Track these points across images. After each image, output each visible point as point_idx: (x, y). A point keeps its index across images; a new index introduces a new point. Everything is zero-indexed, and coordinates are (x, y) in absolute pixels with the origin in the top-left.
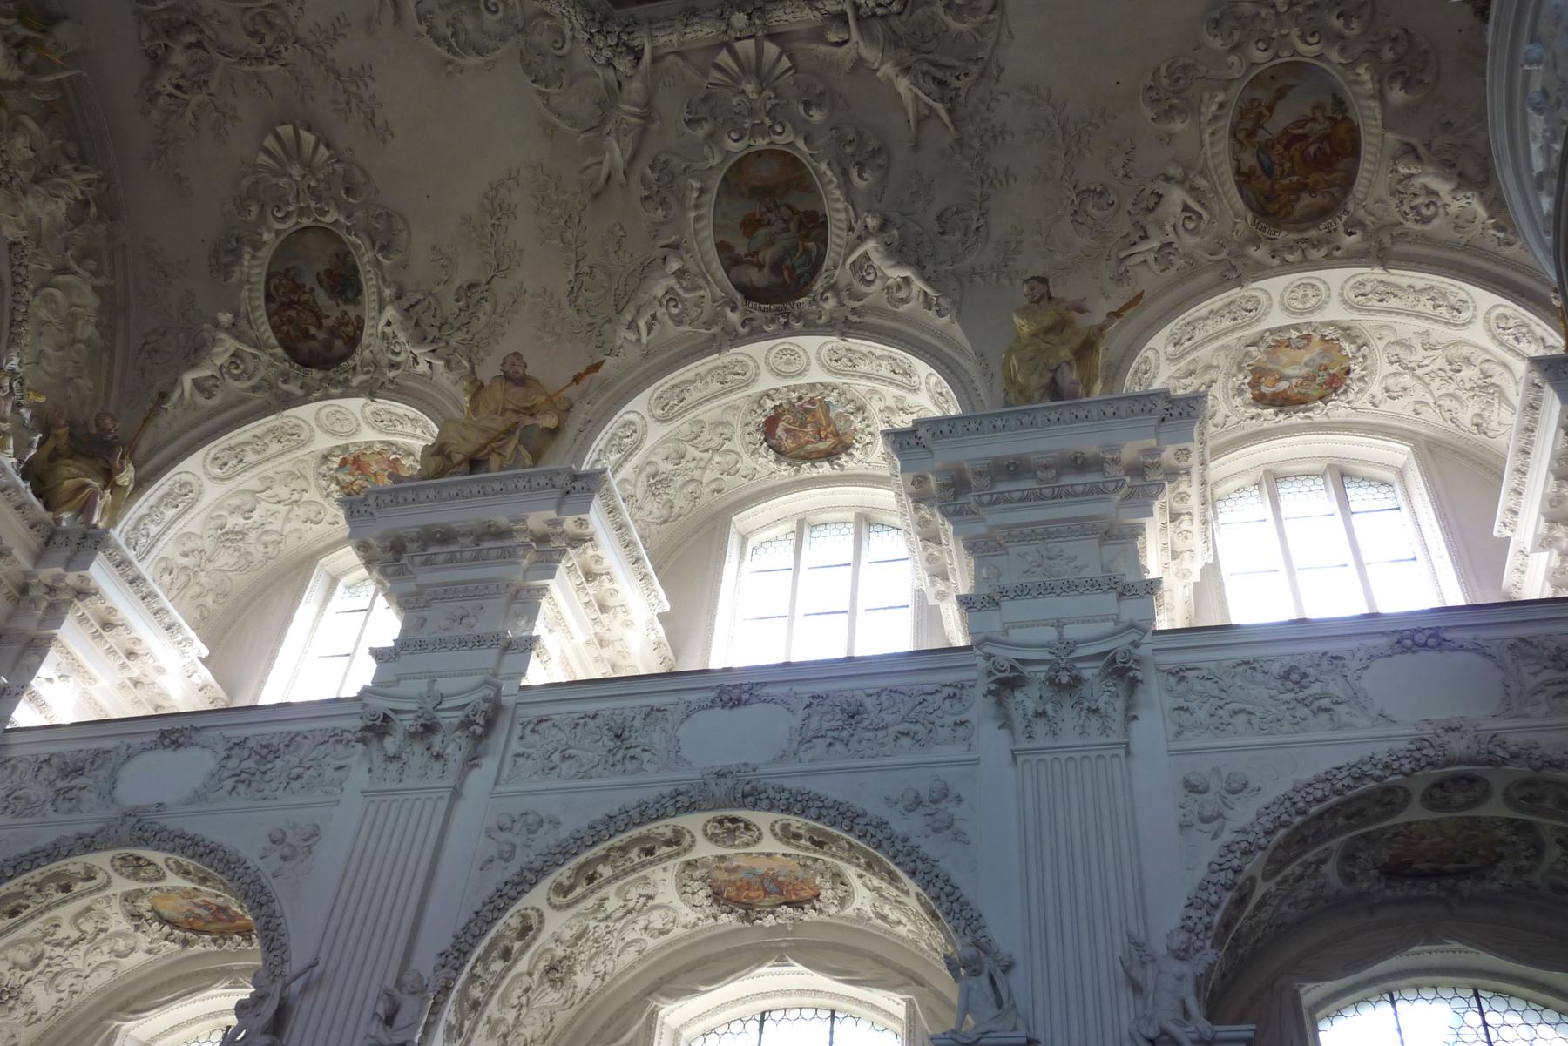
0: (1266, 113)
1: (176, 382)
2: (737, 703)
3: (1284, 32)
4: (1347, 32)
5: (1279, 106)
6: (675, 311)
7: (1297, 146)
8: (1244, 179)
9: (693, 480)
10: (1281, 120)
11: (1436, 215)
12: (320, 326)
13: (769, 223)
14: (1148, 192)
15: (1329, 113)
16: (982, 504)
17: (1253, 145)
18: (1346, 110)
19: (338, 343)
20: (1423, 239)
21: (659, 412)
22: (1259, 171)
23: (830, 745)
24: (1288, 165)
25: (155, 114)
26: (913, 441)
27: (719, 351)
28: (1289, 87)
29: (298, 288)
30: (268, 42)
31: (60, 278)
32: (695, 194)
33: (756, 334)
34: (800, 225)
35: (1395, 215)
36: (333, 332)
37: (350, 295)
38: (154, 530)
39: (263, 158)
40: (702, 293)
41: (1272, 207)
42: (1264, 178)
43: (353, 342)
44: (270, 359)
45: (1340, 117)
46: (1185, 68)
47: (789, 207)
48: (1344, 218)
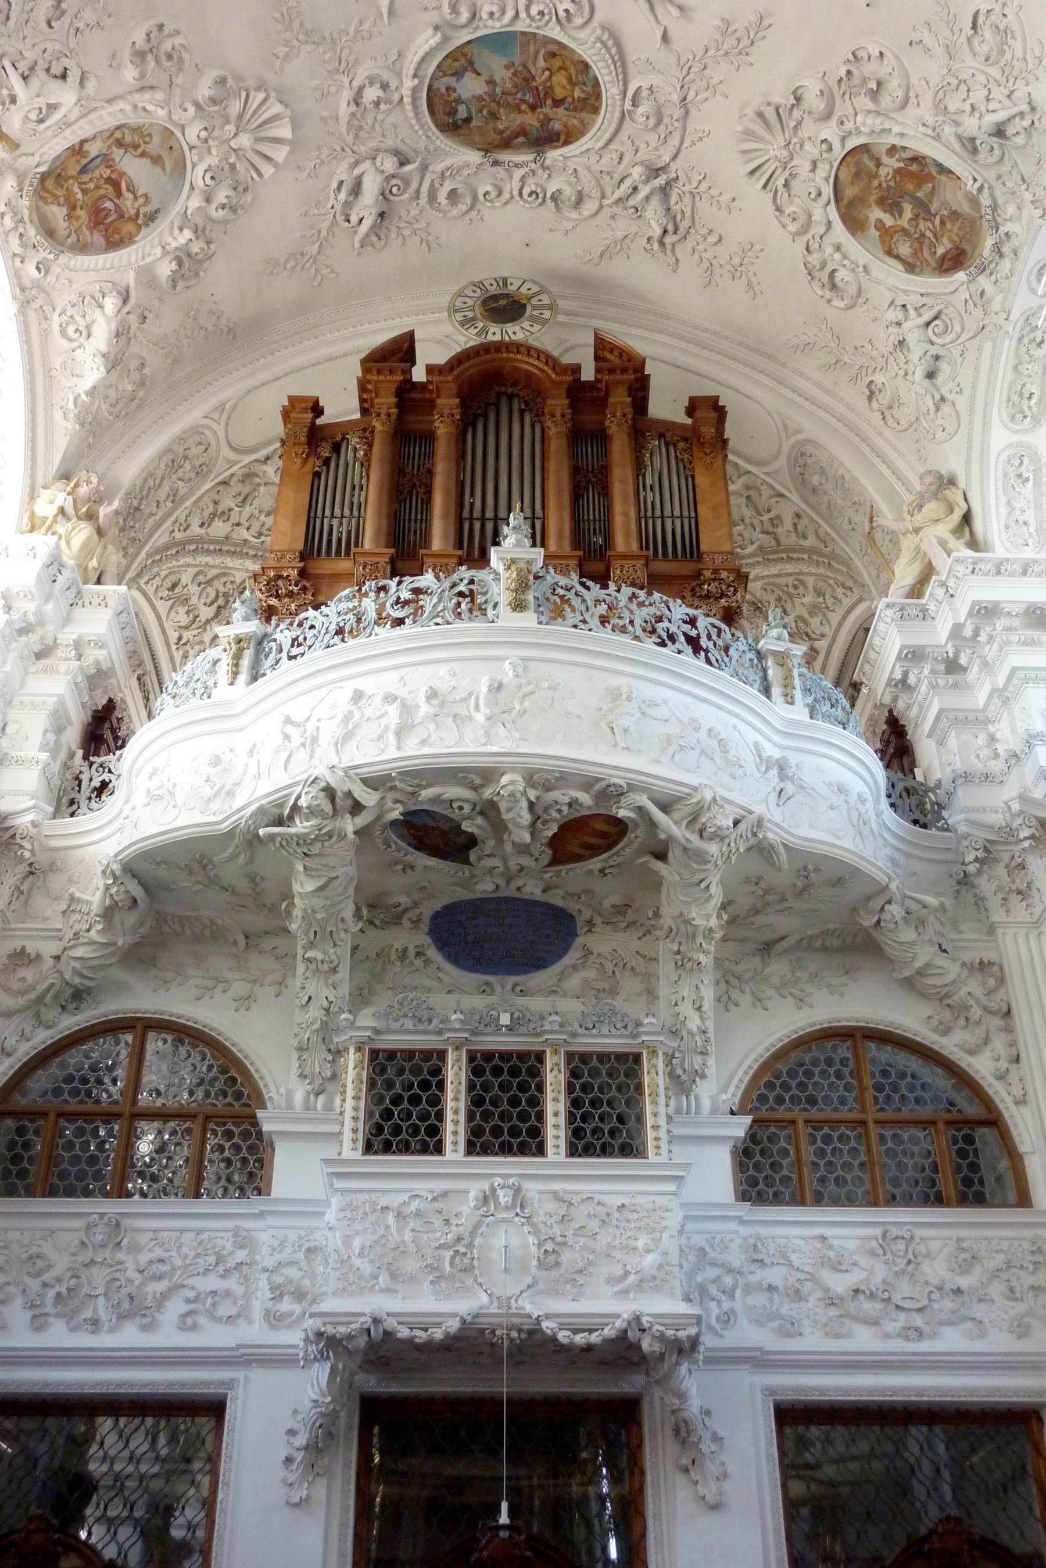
0: (139, 151)
3: (214, 151)
4: (213, 206)
5: (146, 162)
7: (110, 189)
8: (77, 150)
10: (132, 166)
11: (71, 340)
14: (66, 62)
15: (142, 211)
17: (109, 147)
18: (147, 225)
20: (46, 334)
22: (84, 161)
24: (92, 186)
28: (163, 166)
35: (61, 302)
41: (50, 184)
42: (78, 168)
45: (140, 222)
46: (181, 60)
48: (51, 257)
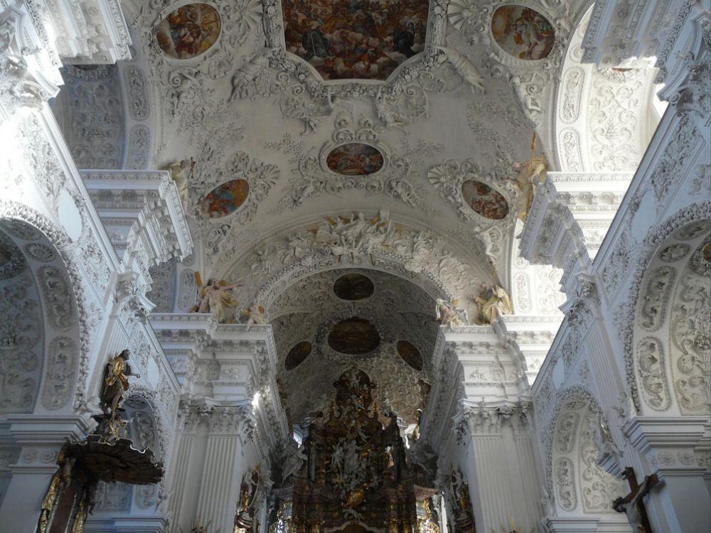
1: (489, 256)
2: (637, 205)
6: (536, 89)
9: (621, 114)
12: (494, 204)
13: (521, 32)
16: (631, 38)
19: (502, 203)
21: (572, 119)
23: (667, 190)
25: (414, 205)
26: (590, 52)
27: (560, 81)
29: (479, 203)
30: (402, 164)
31: (441, 264)
32: (496, 57)
33: (561, 60)
34: (527, 19)
36: (498, 202)
37: (488, 189)
38: (526, 297)
39: (436, 186)
40: (535, 74)
43: (503, 199)
44: (497, 225)
47: (518, 20)
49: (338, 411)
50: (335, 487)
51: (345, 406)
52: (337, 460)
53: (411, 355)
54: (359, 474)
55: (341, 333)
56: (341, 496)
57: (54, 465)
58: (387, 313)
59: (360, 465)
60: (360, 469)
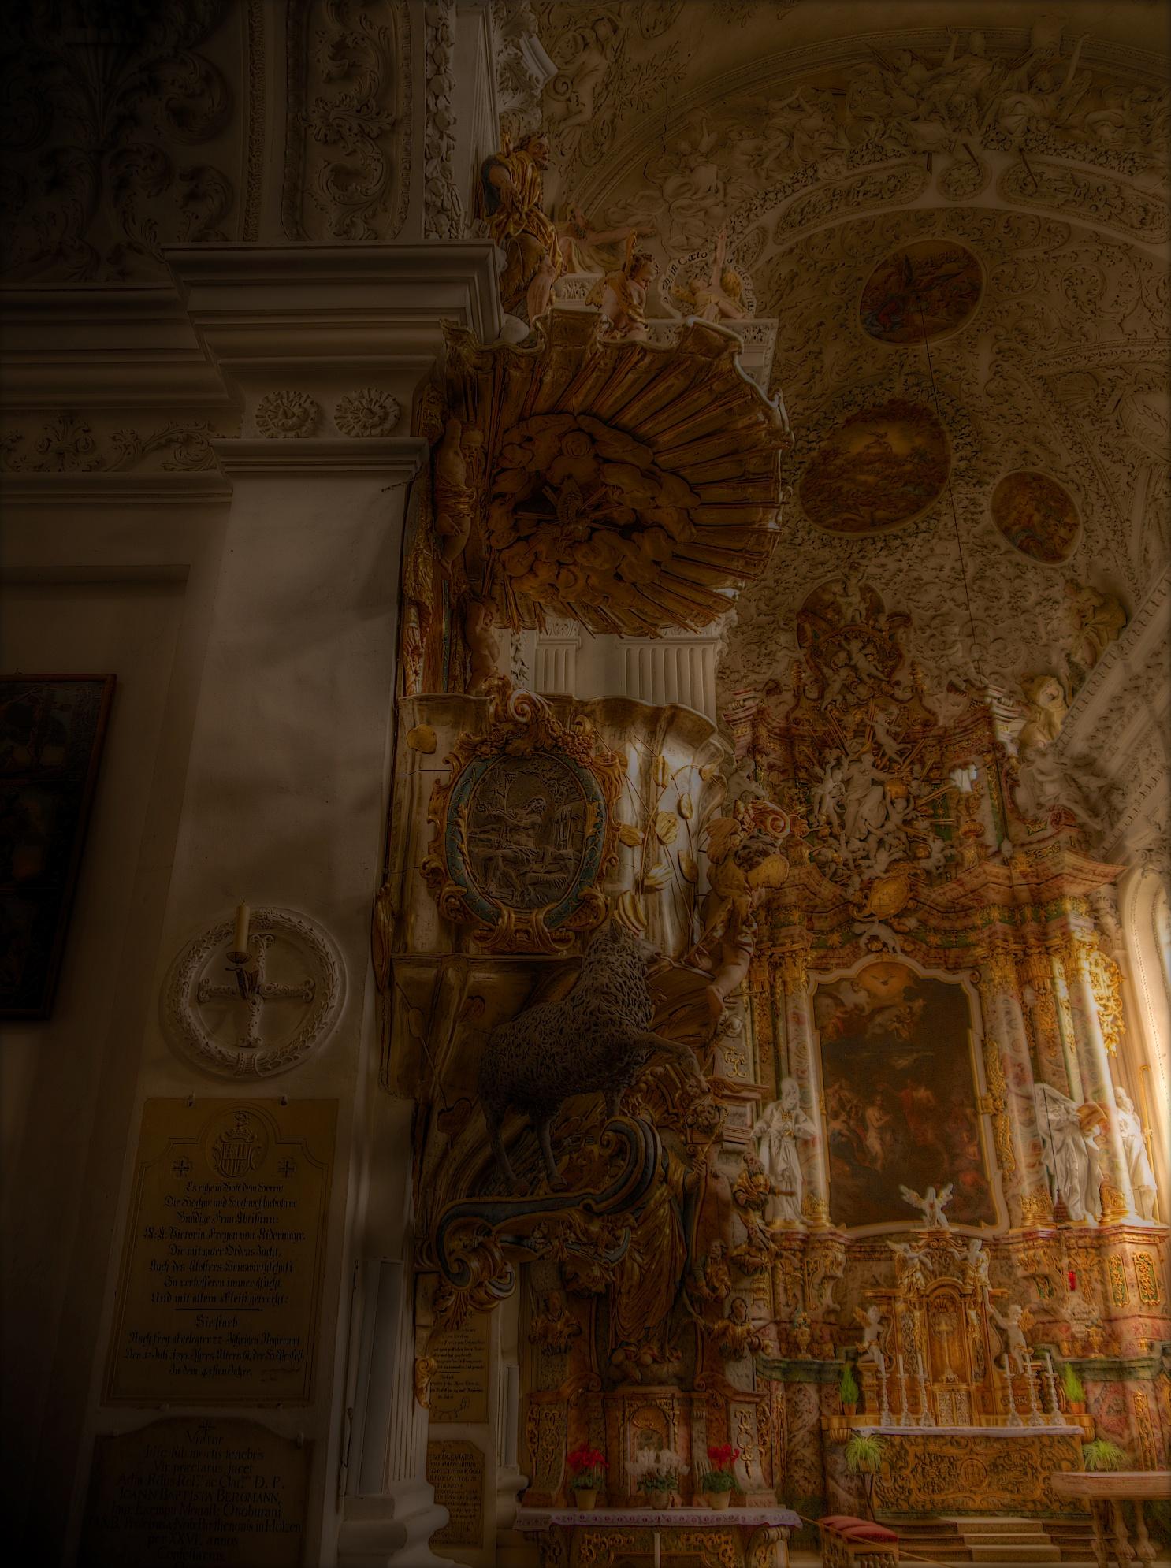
49: (816, 681)
50: (829, 871)
51: (836, 672)
52: (829, 803)
53: (1037, 518)
54: (889, 840)
55: (838, 462)
56: (851, 890)
57: (421, 440)
58: (992, 387)
59: (887, 817)
60: (890, 826)
